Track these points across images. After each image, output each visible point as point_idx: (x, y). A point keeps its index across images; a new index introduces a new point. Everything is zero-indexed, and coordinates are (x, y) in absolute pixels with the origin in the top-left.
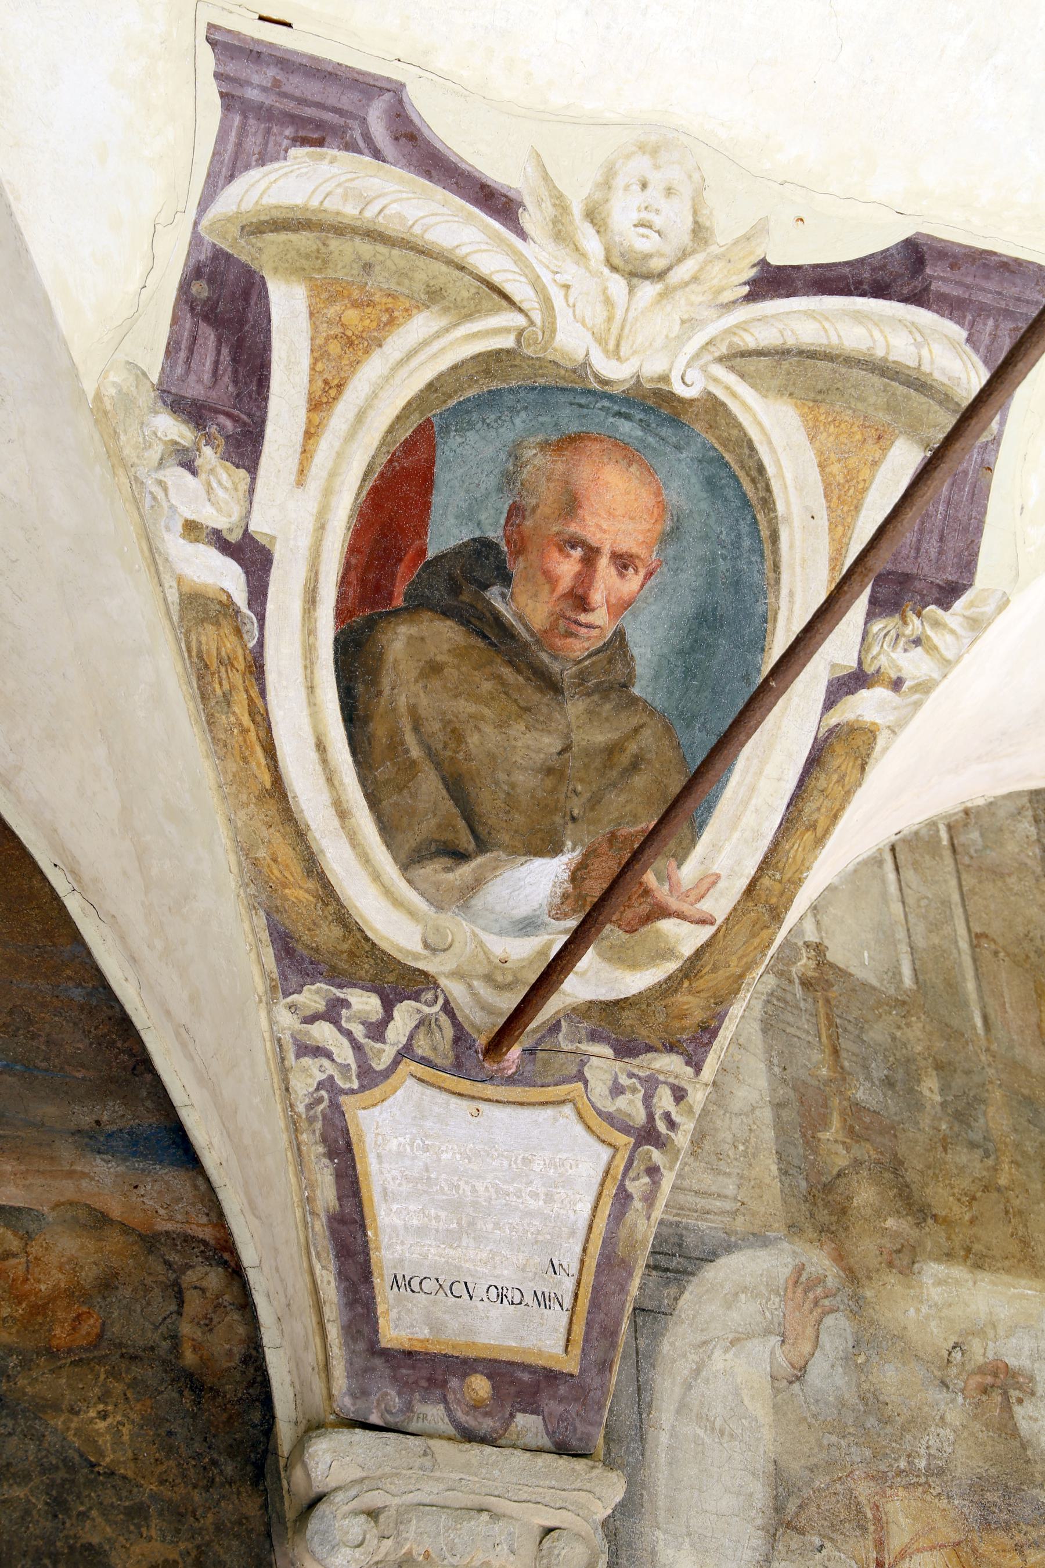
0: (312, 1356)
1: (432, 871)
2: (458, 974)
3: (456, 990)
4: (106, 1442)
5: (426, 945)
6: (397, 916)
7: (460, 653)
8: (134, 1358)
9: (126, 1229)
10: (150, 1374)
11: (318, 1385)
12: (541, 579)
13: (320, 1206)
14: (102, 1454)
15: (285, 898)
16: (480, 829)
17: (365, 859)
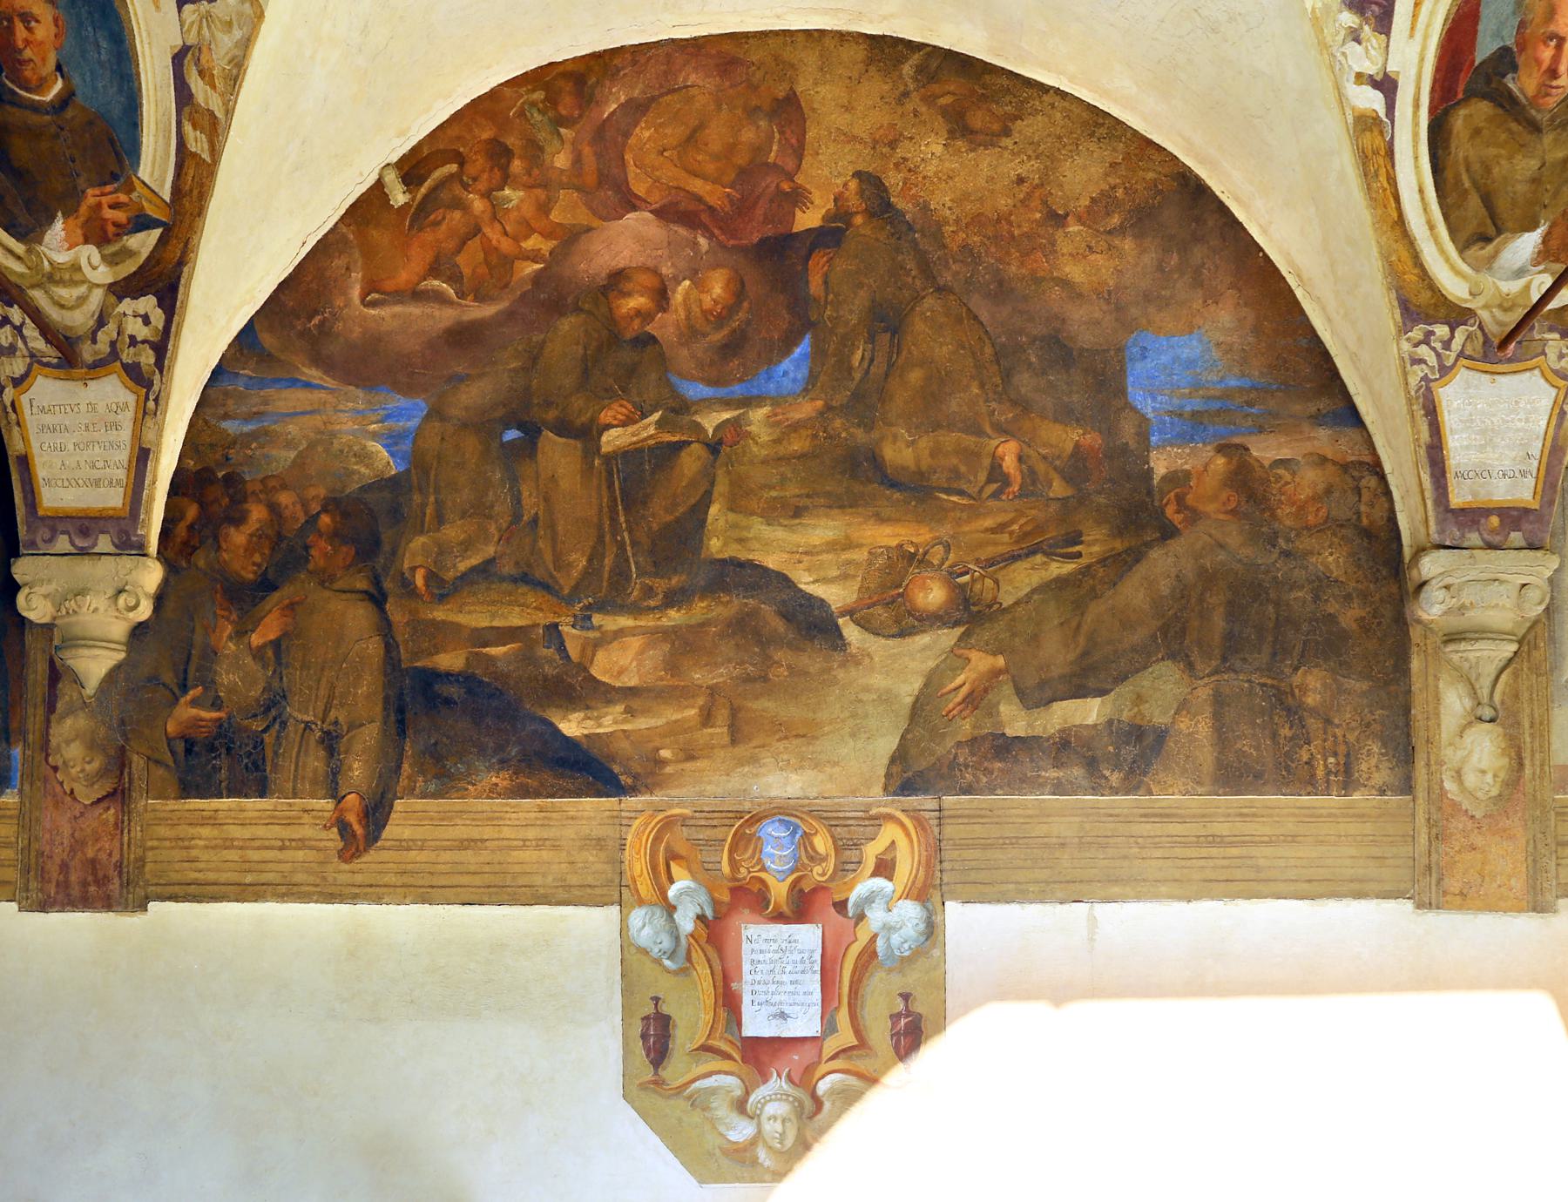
0: (1419, 516)
1: (1475, 251)
2: (1486, 307)
3: (1484, 315)
4: (1333, 567)
5: (1471, 294)
6: (1457, 280)
7: (1490, 120)
8: (1342, 526)
9: (1334, 463)
10: (1348, 532)
11: (1423, 530)
12: (1534, 63)
13: (1422, 441)
14: (1332, 572)
15: (1404, 280)
16: (1499, 223)
17: (1442, 251)
